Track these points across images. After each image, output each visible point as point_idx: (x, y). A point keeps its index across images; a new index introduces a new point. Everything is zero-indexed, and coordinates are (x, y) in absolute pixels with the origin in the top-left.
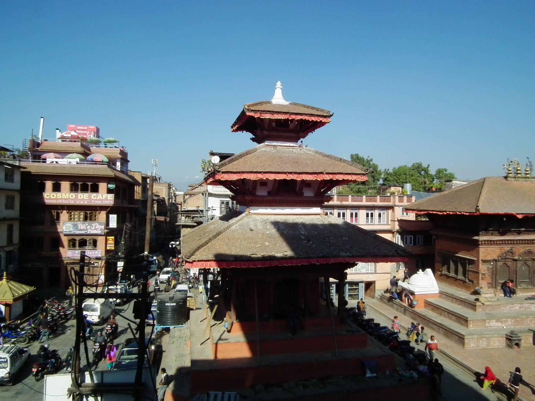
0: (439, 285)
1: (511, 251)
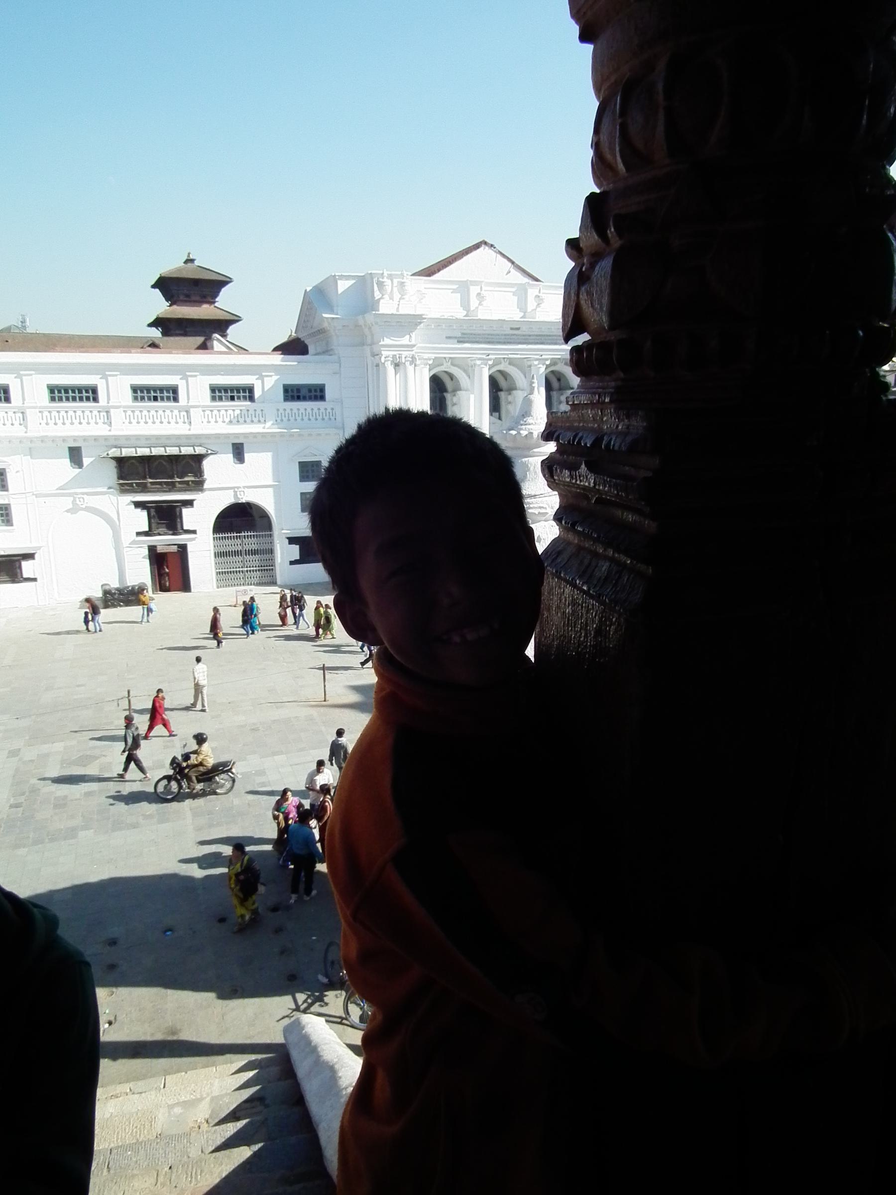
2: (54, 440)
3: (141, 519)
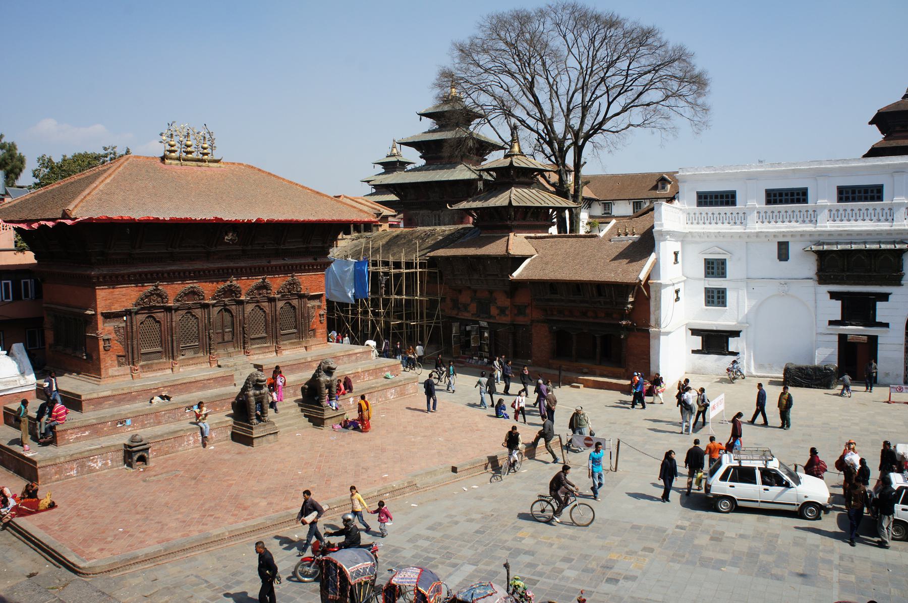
0: (37, 372)
1: (158, 292)
2: (766, 235)
3: (835, 309)
